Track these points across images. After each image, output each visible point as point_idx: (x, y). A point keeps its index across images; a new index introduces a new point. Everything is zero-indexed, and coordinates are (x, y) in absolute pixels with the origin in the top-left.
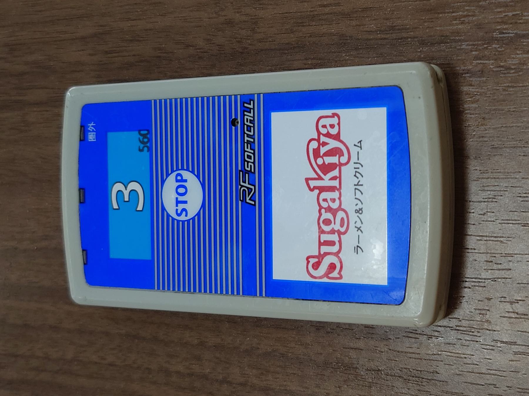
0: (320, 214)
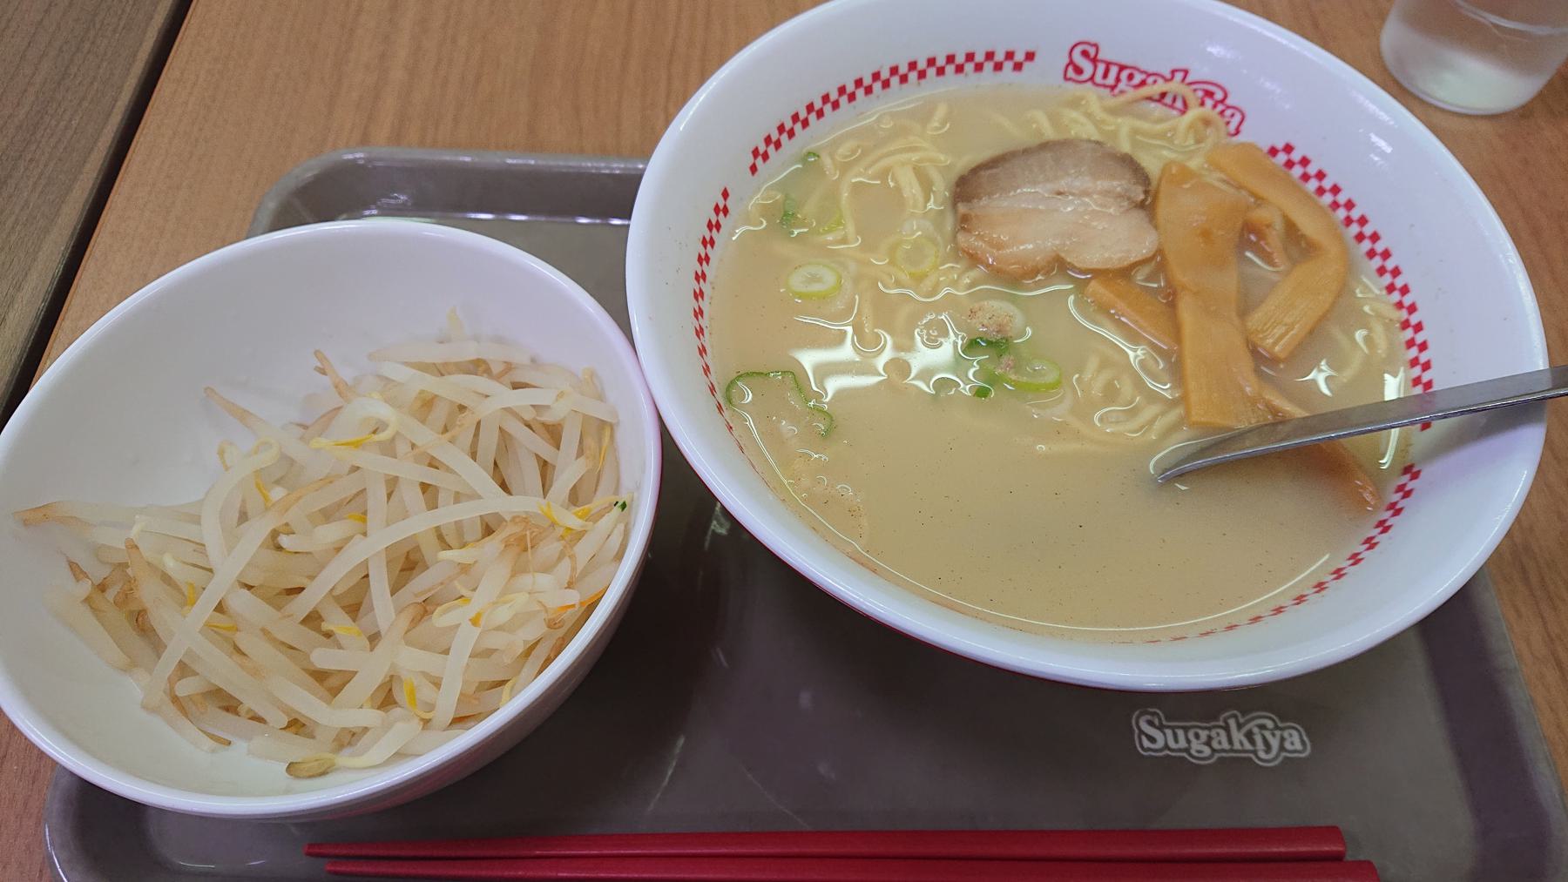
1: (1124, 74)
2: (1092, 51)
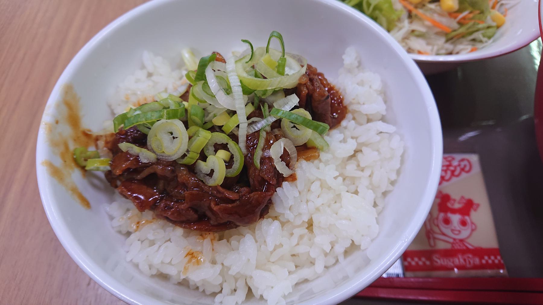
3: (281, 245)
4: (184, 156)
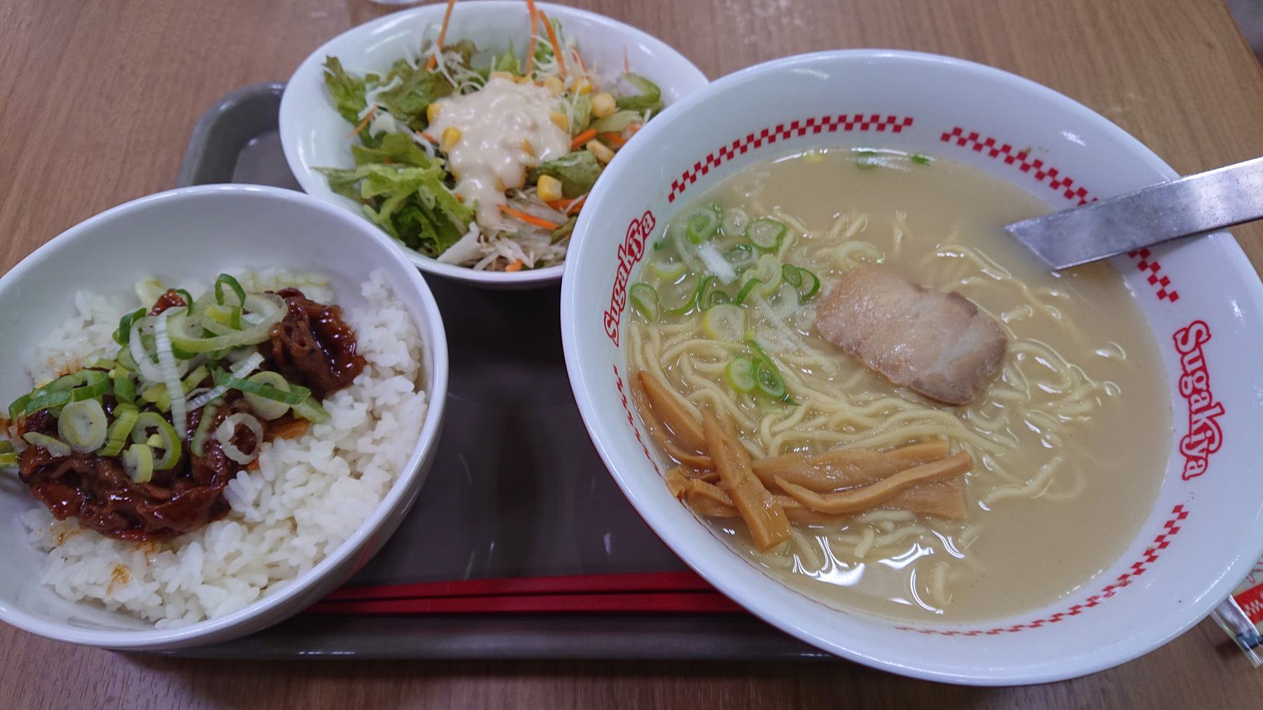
0: (1207, 384)
1: (1200, 374)
2: (1204, 337)
3: (238, 553)
4: (104, 445)
